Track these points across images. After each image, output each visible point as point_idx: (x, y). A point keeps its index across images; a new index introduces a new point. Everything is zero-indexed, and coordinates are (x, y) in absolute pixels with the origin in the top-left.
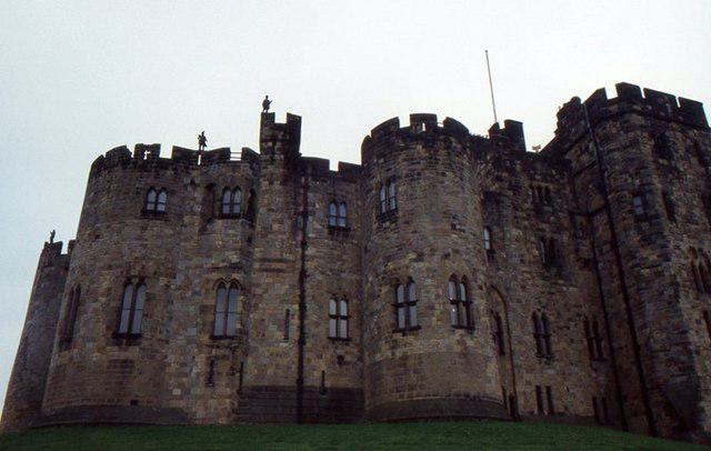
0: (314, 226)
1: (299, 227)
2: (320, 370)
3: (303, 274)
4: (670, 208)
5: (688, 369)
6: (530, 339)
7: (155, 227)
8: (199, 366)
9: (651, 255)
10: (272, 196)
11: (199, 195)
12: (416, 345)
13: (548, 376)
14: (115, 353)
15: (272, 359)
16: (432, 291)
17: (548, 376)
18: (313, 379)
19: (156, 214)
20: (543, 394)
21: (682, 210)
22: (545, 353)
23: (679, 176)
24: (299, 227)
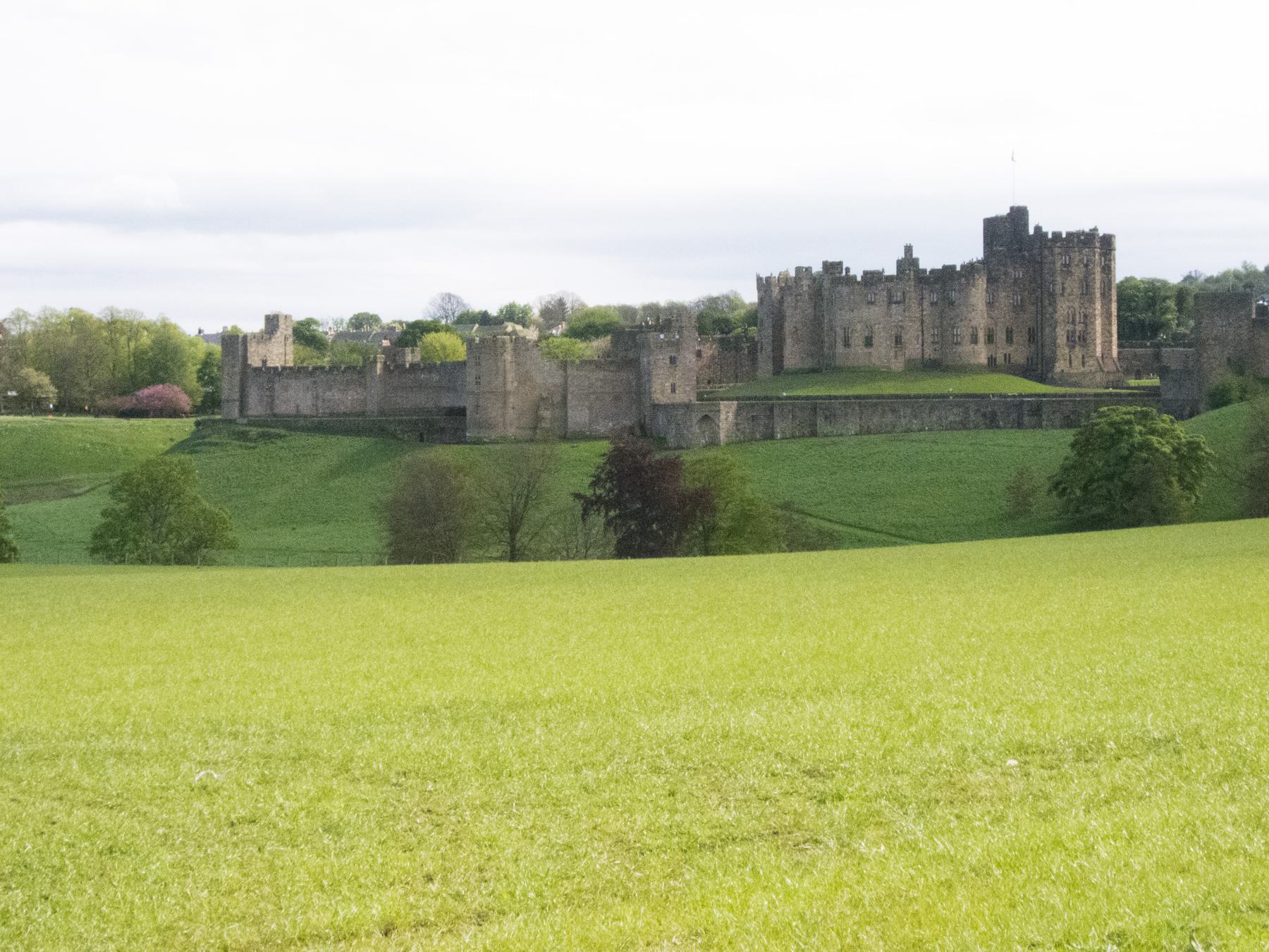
0: (926, 304)
1: (921, 304)
2: (929, 353)
3: (922, 322)
4: (1063, 289)
5: (1054, 352)
6: (1004, 337)
7: (873, 307)
8: (892, 354)
9: (1050, 309)
10: (913, 294)
11: (885, 293)
12: (960, 349)
13: (1010, 350)
14: (866, 350)
15: (913, 349)
16: (963, 331)
17: (1010, 350)
18: (926, 356)
19: (872, 303)
20: (1007, 357)
21: (1068, 290)
22: (1009, 340)
23: (1070, 273)
24: (921, 304)
